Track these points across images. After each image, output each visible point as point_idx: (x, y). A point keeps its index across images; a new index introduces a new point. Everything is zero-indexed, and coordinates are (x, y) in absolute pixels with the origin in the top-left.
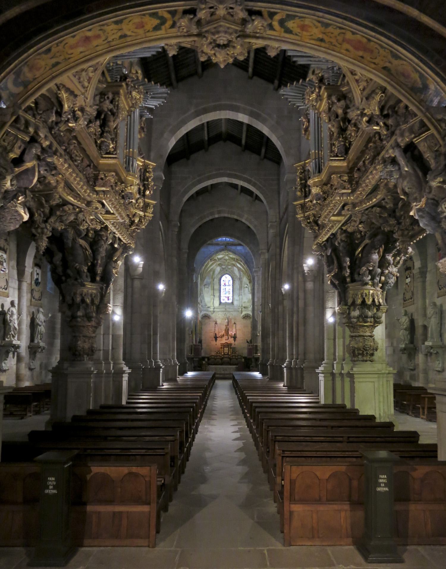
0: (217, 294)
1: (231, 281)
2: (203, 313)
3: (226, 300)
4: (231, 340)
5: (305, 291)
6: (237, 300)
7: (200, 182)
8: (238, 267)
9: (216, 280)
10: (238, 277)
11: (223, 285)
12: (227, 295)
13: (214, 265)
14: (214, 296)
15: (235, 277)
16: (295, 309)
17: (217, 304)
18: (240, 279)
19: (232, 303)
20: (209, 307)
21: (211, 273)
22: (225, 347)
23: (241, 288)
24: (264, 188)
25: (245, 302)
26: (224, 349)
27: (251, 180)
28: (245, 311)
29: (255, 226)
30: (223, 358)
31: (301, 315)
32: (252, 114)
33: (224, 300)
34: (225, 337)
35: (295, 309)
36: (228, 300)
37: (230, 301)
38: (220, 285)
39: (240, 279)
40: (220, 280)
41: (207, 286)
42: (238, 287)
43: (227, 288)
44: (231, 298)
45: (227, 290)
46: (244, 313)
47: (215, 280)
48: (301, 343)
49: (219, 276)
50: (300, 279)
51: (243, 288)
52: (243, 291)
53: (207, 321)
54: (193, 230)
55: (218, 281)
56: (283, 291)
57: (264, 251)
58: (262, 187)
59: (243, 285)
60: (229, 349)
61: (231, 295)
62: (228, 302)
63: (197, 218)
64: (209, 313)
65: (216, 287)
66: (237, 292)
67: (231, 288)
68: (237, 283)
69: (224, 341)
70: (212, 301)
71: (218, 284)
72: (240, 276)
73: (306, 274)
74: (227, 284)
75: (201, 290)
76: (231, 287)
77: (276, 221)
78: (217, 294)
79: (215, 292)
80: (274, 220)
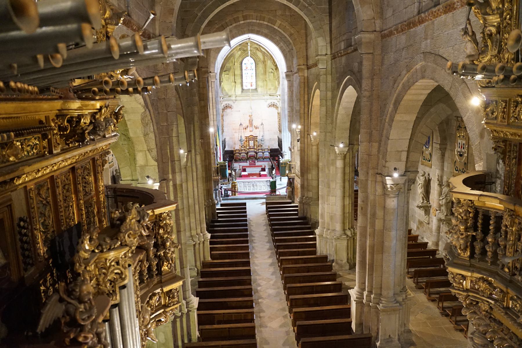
0: (238, 81)
3: (249, 87)
9: (237, 65)
13: (235, 50)
14: (235, 82)
15: (258, 60)
19: (256, 89)
20: (230, 96)
22: (250, 140)
23: (265, 72)
24: (310, 8)
28: (271, 99)
29: (291, 35)
34: (248, 128)
37: (254, 87)
38: (241, 69)
39: (264, 62)
41: (227, 72)
42: (262, 72)
44: (254, 84)
46: (269, 102)
47: (236, 64)
49: (240, 60)
51: (267, 73)
53: (228, 111)
55: (239, 66)
58: (307, 5)
59: (268, 69)
62: (251, 88)
63: (217, 27)
64: (230, 103)
65: (238, 72)
68: (261, 66)
70: (234, 88)
71: (239, 69)
72: (264, 58)
73: (389, 189)
74: (249, 68)
77: (326, 54)
78: (238, 81)
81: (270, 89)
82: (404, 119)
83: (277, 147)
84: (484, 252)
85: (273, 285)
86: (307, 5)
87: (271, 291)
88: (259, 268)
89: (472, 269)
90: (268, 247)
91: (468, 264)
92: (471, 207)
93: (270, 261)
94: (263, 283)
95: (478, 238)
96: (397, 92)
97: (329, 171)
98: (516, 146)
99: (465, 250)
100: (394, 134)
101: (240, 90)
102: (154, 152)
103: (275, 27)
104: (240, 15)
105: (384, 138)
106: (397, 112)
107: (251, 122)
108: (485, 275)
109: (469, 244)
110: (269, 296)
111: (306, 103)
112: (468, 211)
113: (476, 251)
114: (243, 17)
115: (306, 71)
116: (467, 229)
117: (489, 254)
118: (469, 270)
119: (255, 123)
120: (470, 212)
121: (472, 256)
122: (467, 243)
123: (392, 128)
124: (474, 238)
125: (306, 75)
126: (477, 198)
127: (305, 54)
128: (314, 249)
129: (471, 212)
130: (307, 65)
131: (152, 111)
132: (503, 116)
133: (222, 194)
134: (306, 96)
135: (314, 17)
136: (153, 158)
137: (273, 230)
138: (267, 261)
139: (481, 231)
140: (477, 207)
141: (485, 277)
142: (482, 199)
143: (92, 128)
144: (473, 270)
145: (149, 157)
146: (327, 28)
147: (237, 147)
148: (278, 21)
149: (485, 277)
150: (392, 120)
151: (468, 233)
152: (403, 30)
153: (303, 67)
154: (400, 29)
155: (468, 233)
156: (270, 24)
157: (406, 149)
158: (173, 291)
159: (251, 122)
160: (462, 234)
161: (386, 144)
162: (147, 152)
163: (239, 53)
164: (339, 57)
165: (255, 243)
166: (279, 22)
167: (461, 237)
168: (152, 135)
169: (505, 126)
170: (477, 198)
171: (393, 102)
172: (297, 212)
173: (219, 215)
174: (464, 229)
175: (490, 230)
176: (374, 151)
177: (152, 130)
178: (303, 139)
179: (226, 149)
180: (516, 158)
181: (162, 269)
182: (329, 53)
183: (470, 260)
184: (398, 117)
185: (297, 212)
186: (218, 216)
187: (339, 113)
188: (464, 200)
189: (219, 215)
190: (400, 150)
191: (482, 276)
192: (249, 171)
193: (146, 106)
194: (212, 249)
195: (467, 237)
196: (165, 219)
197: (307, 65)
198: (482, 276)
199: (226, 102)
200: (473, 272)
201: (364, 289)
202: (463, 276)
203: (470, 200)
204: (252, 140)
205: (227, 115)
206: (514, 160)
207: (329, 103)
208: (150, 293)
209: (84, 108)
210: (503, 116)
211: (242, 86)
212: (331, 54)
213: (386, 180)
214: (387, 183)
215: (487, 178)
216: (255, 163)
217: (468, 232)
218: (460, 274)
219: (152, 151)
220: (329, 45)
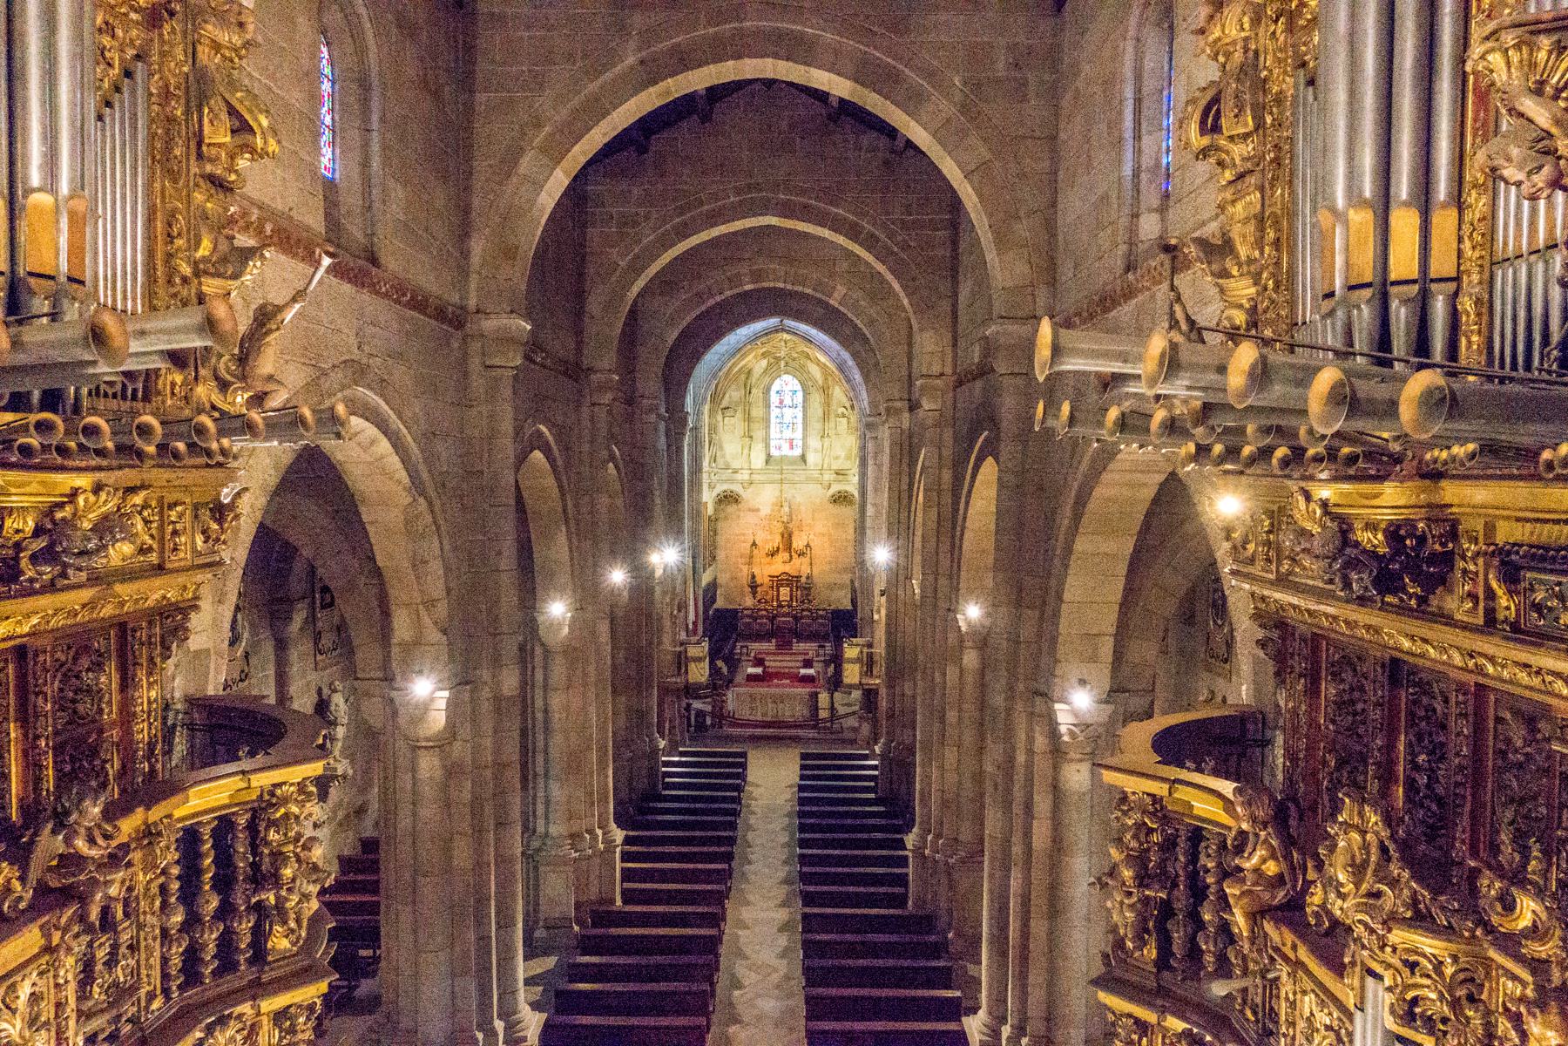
1: (800, 395)
2: (720, 488)
3: (786, 451)
4: (800, 566)
5: (1056, 788)
6: (816, 451)
7: (683, 232)
8: (818, 363)
9: (757, 393)
10: (820, 382)
11: (777, 404)
12: (788, 434)
13: (750, 357)
16: (1017, 850)
17: (758, 460)
18: (825, 390)
20: (735, 472)
21: (743, 377)
23: (826, 417)
24: (902, 255)
25: (837, 458)
26: (778, 591)
27: (857, 224)
29: (871, 323)
30: (774, 617)
31: (1039, 875)
32: (864, 74)
33: (780, 449)
35: (1017, 850)
36: (791, 447)
37: (797, 452)
39: (825, 390)
40: (767, 390)
43: (788, 413)
45: (787, 419)
46: (835, 488)
47: (754, 391)
48: (1036, 977)
50: (1041, 742)
51: (832, 416)
52: (832, 425)
53: (731, 509)
54: (672, 335)
56: (961, 623)
57: (898, 404)
58: (896, 249)
60: (791, 591)
61: (799, 434)
64: (737, 488)
65: (757, 412)
66: (816, 425)
67: (800, 415)
68: (816, 399)
69: (778, 566)
70: (746, 451)
74: (787, 401)
75: (713, 429)
76: (799, 413)
77: (942, 374)
78: (758, 434)
79: (754, 426)
80: (936, 369)
81: (837, 458)
82: (1102, 550)
83: (850, 607)
84: (1194, 953)
85: (778, 987)
86: (896, 249)
87: (769, 1005)
88: (747, 932)
89: (1159, 1002)
90: (782, 874)
91: (1151, 983)
92: (1154, 814)
93: (782, 915)
94: (749, 977)
95: (1181, 910)
96: (1079, 476)
97: (944, 674)
98: (1305, 641)
99: (1141, 943)
100: (1075, 588)
101: (763, 457)
102: (442, 609)
103: (832, 302)
104: (744, 269)
105: (1051, 599)
106: (1081, 530)
107: (787, 538)
108: (1198, 1025)
109: (1151, 924)
110: (759, 1018)
111: (905, 495)
112: (1145, 824)
113: (1175, 949)
114: (752, 273)
115: (907, 415)
116: (1142, 880)
117: (1209, 958)
118: (1150, 1005)
119: (798, 543)
120: (1150, 831)
121: (1163, 962)
122: (1145, 920)
123: (1070, 572)
124: (1167, 910)
125: (906, 425)
126: (1166, 786)
127: (904, 372)
128: (902, 890)
129: (1156, 830)
130: (909, 400)
131: (437, 503)
132: (1267, 555)
133: (689, 725)
134: (905, 479)
135: (914, 279)
136: (436, 623)
137: (802, 828)
138: (773, 915)
139: (1185, 886)
140: (1172, 815)
141: (1195, 1030)
142: (1183, 793)
143: (44, 544)
144: (1163, 1006)
145: (427, 621)
146: (946, 306)
147: (749, 602)
148: (839, 287)
149: (1195, 1030)
150: (1069, 550)
151: (1147, 893)
152: (1092, 316)
153: (898, 404)
154: (1085, 314)
155: (1147, 893)
156: (818, 295)
157: (1112, 630)
158: (292, 1010)
159: (787, 538)
160: (1130, 894)
161: (1056, 614)
162: (421, 607)
163: (764, 363)
164: (969, 381)
165: (750, 863)
166: (841, 290)
167: (1126, 901)
168: (436, 567)
169: (1271, 583)
170: (1166, 786)
171: (1071, 501)
172: (872, 784)
173: (667, 780)
174: (1135, 878)
175: (1208, 887)
176: (1027, 631)
177: (438, 552)
178: (894, 590)
179: (715, 606)
180: (1305, 676)
181: (269, 945)
182: (948, 370)
183: (1159, 971)
184: (1081, 545)
185: (872, 784)
186: (663, 783)
187: (967, 524)
188: (1134, 793)
189: (667, 780)
190: (1094, 632)
191: (1189, 1026)
192: (773, 663)
193: (417, 485)
194: (628, 875)
195: (1146, 901)
196: (285, 800)
197: (909, 400)
198: (1189, 1026)
199: (725, 487)
200: (1163, 1011)
201: (1002, 1020)
202: (1137, 1021)
203: (1148, 794)
204: (787, 585)
205: (726, 518)
206: (1302, 681)
207: (947, 499)
208: (210, 1016)
209: (13, 490)
210: (1267, 555)
211: (767, 446)
212: (954, 373)
213: (1054, 711)
214: (1059, 721)
215: (1251, 727)
216: (790, 643)
217: (1147, 887)
218: (1130, 1016)
219: (433, 606)
220: (949, 350)
